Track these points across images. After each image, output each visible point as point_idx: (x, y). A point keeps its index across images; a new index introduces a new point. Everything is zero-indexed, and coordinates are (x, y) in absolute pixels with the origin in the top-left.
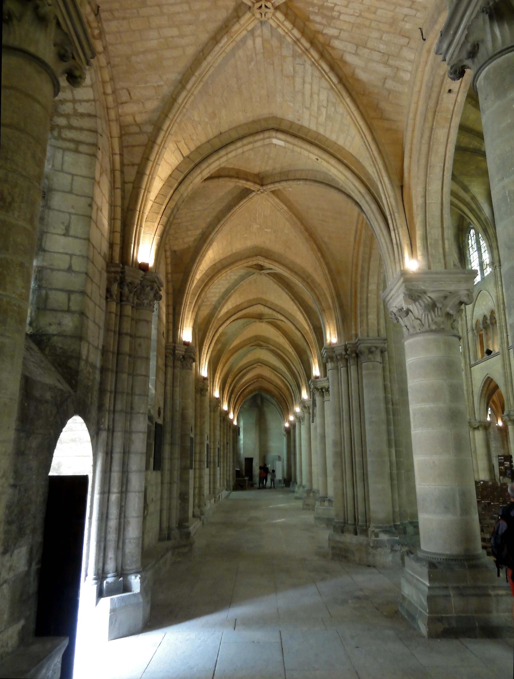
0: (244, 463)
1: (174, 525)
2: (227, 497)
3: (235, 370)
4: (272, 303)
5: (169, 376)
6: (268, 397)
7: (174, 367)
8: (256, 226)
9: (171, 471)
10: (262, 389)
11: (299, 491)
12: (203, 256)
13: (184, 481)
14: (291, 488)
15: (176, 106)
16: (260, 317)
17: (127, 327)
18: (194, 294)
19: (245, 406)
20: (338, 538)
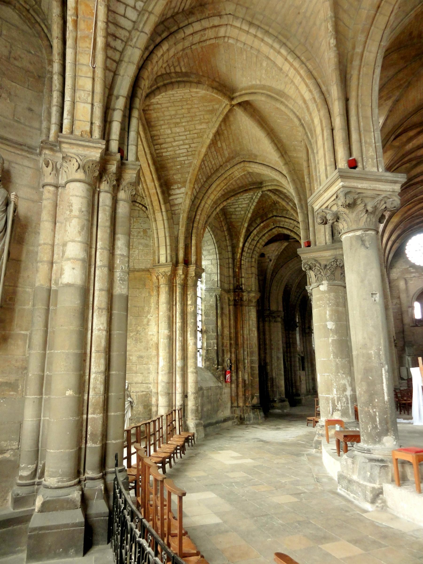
1: (311, 388)
9: (308, 371)
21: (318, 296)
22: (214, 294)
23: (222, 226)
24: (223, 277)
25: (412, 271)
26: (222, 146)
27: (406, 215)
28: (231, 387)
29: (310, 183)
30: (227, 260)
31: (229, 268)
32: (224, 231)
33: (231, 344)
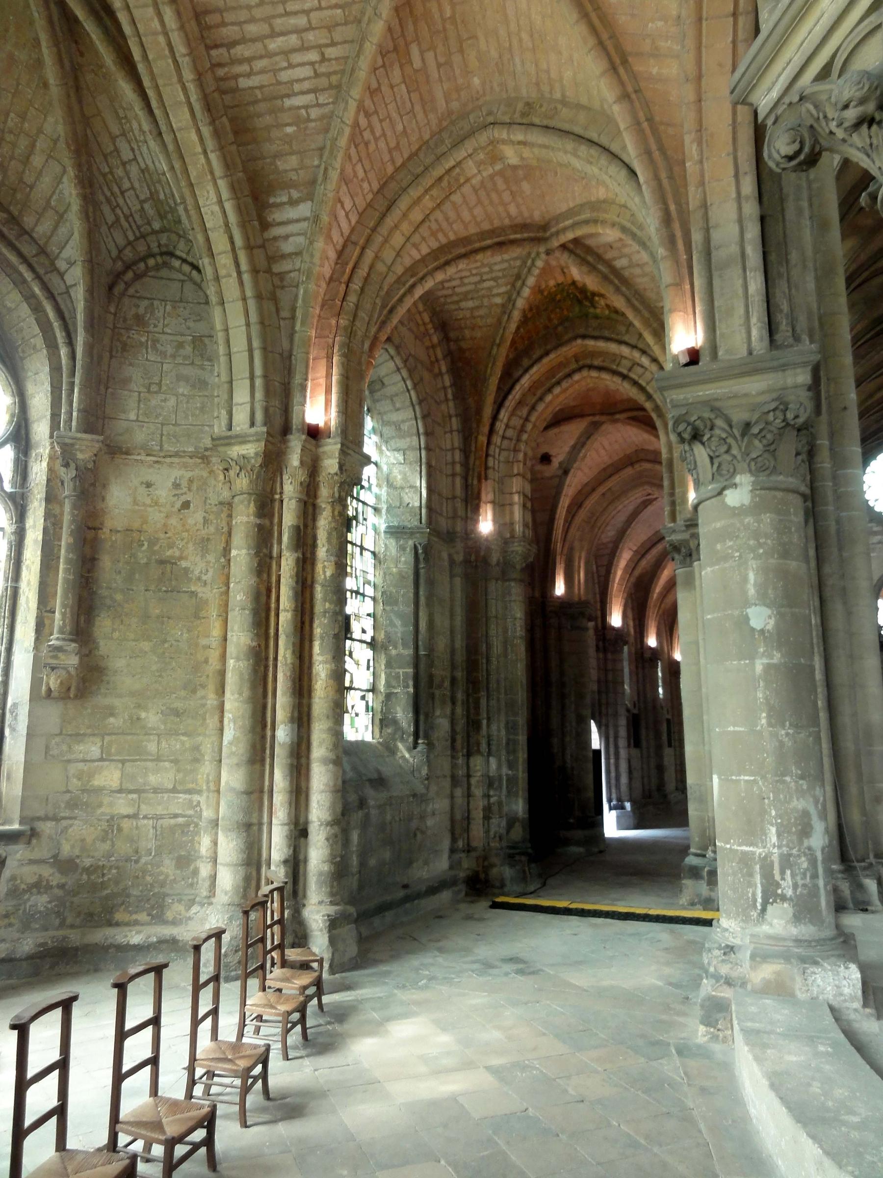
5: (640, 675)
7: (643, 668)
17: (610, 667)
18: (655, 606)
21: (718, 525)
22: (411, 543)
23: (437, 360)
24: (435, 497)
25: (875, 529)
26: (424, 68)
27: (870, 402)
28: (452, 797)
29: (701, 162)
30: (449, 454)
31: (454, 475)
32: (441, 374)
33: (453, 680)
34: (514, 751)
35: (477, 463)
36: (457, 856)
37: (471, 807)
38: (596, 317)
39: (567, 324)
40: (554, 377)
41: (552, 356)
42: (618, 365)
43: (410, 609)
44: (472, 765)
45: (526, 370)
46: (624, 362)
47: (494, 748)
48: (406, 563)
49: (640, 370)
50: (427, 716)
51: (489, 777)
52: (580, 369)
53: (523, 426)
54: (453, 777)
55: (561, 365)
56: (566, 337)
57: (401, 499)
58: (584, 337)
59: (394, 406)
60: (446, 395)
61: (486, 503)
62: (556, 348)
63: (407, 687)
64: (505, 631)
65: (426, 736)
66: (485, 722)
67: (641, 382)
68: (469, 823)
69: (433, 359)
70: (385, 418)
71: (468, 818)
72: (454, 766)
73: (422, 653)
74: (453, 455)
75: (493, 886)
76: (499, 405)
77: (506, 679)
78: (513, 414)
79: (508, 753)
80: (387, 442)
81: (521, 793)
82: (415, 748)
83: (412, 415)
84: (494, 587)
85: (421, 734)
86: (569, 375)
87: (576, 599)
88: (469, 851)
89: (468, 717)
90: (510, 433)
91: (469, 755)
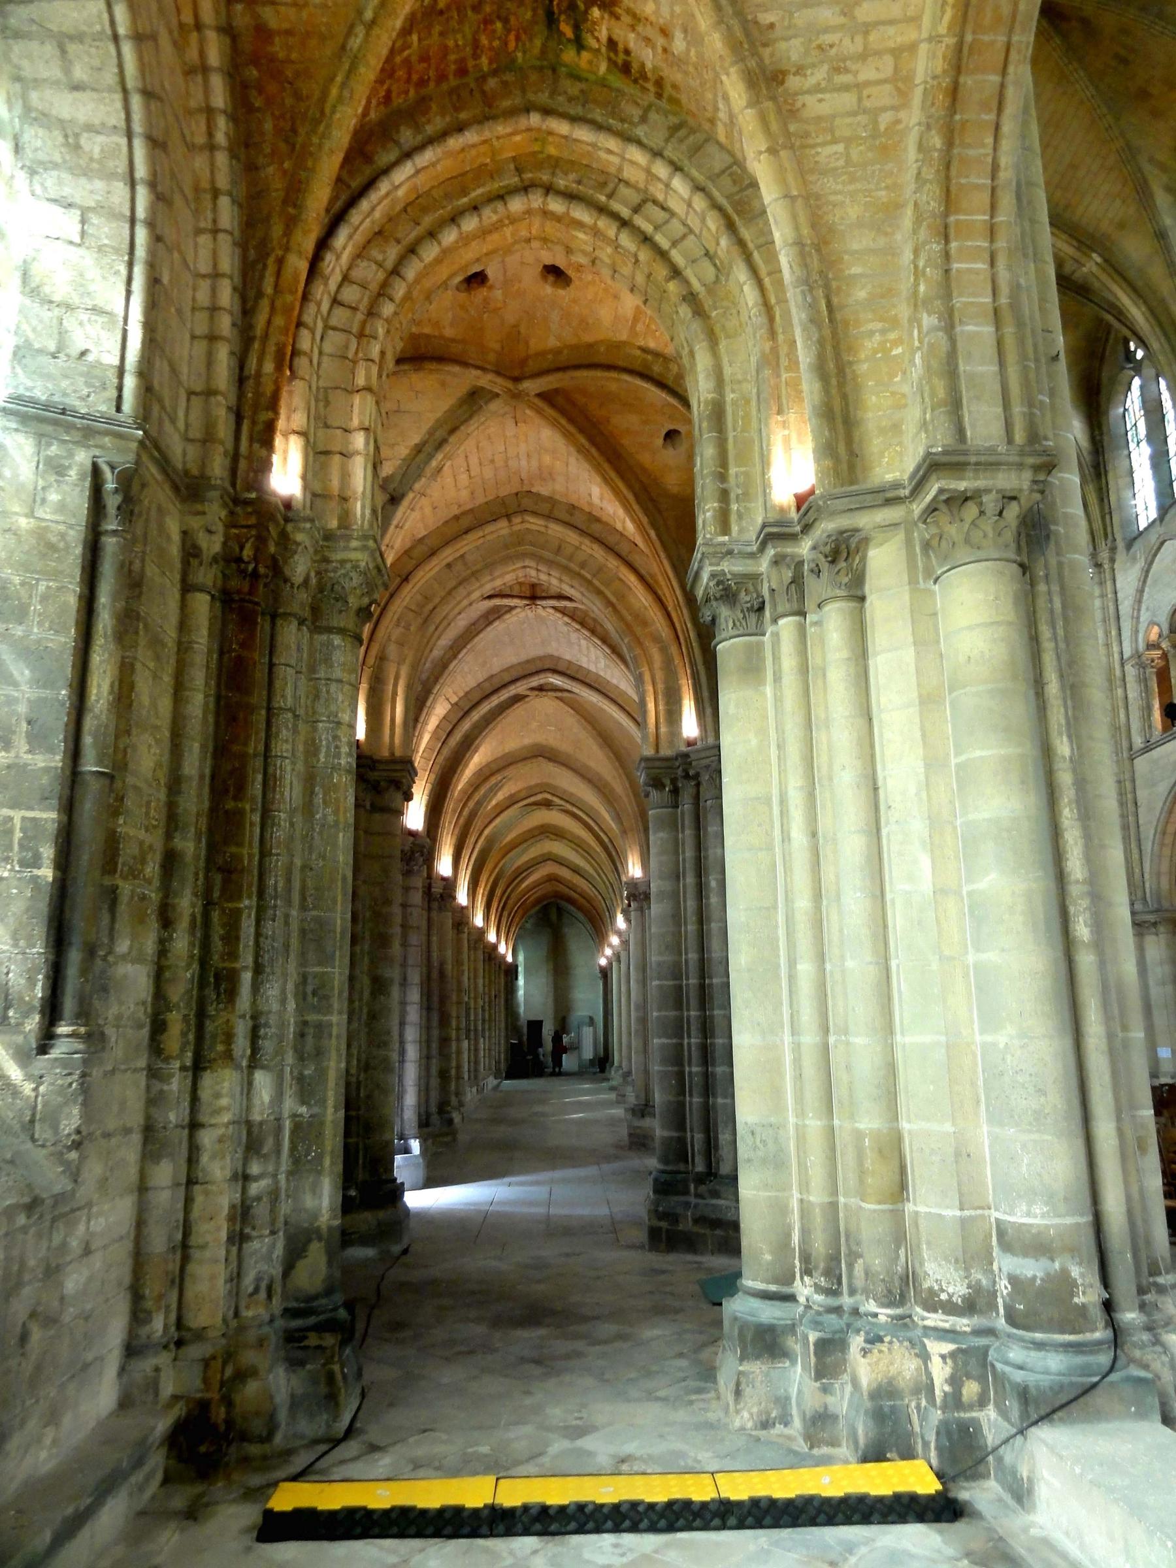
0: (525, 1030)
2: (496, 1088)
3: (509, 872)
4: (565, 791)
6: (572, 908)
8: (534, 724)
10: (558, 895)
11: (615, 1077)
12: (466, 765)
13: (444, 1055)
14: (606, 1074)
15: (447, 672)
16: (547, 804)
18: (454, 811)
19: (528, 926)
20: (637, 1123)
22: (83, 457)
23: (198, 26)
28: (143, 1188)
30: (205, 286)
31: (212, 338)
32: (205, 69)
33: (170, 861)
34: (319, 1053)
35: (279, 321)
36: (146, 1365)
37: (196, 1212)
38: (575, 77)
39: (509, 77)
40: (464, 192)
41: (471, 137)
42: (610, 196)
43: (67, 638)
44: (205, 1094)
45: (408, 155)
46: (624, 191)
47: (268, 1046)
48: (61, 507)
49: (659, 215)
50: (91, 951)
51: (249, 1124)
52: (525, 189)
53: (385, 285)
54: (149, 1130)
55: (482, 173)
56: (506, 103)
57: (62, 334)
58: (547, 112)
59: (67, 71)
60: (210, 134)
61: (286, 435)
62: (483, 120)
63: (36, 862)
64: (312, 749)
65: (84, 1014)
66: (247, 977)
67: (659, 239)
68: (185, 1259)
69: (188, 18)
70: (34, 96)
71: (185, 1248)
72: (154, 1101)
73: (90, 766)
74: (214, 291)
75: (244, 1437)
76: (336, 221)
77: (306, 867)
78: (360, 254)
79: (301, 1057)
80: (33, 172)
81: (327, 1162)
82: (43, 1050)
83: (118, 119)
84: (291, 636)
85: (69, 1004)
86: (501, 197)
87: (385, 753)
88: (179, 1343)
89: (204, 962)
90: (350, 294)
91: (198, 1067)
